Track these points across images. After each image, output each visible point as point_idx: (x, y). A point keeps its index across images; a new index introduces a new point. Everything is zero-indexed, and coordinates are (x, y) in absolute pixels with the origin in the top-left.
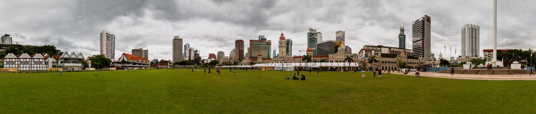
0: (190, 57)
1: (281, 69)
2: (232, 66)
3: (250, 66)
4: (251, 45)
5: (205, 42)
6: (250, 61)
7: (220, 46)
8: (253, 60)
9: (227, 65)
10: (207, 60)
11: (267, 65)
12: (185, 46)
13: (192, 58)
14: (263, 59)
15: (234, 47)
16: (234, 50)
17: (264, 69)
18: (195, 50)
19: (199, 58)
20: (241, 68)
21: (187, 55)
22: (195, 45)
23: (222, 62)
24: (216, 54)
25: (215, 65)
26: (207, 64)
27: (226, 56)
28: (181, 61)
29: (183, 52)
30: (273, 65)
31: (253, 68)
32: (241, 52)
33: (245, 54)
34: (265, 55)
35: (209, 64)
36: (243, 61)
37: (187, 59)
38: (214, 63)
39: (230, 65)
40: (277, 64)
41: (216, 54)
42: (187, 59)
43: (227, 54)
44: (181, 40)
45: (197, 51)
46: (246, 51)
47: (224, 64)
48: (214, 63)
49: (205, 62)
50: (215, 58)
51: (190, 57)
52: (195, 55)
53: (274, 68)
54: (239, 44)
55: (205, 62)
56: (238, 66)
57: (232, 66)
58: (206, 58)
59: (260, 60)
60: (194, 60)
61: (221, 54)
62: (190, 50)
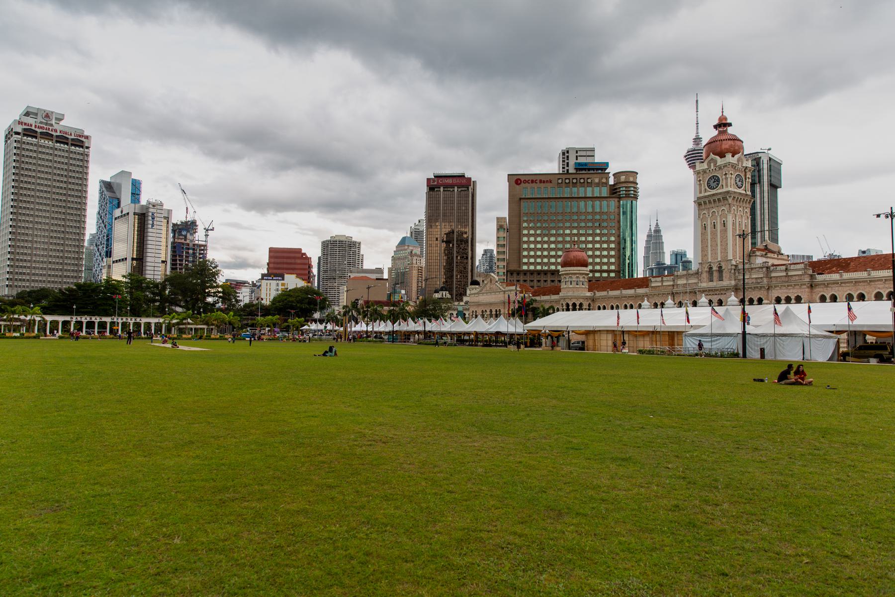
0: (140, 259)
1: (735, 345)
2: (411, 326)
3: (515, 327)
4: (516, 201)
5: (246, 173)
6: (514, 294)
7: (332, 206)
8: (535, 290)
9: (383, 318)
10: (255, 286)
11: (628, 319)
12: (108, 187)
13: (157, 269)
14: (594, 284)
15: (423, 217)
16: (416, 234)
17: (606, 343)
18: (178, 217)
19: (205, 272)
20: (460, 339)
21: (123, 248)
22: (174, 181)
23: (344, 300)
24: (314, 253)
25: (306, 314)
26: (252, 311)
27: (368, 265)
28: (68, 284)
29: (91, 227)
30: (673, 317)
31: (534, 339)
32: (458, 246)
33: (480, 250)
34: (604, 262)
35: (266, 311)
36: (472, 294)
37: (119, 273)
38: (299, 302)
39: (394, 317)
40: (701, 317)
41: (314, 253)
42: (119, 273)
43: (378, 255)
44: (79, 142)
45: (190, 226)
46: (486, 240)
47: (356, 311)
48: (296, 308)
49: (244, 297)
50: (308, 277)
51: (140, 259)
52: (177, 250)
53: (673, 336)
54: (450, 195)
55: (244, 297)
56: (446, 326)
57: (411, 326)
58: (252, 275)
59: (574, 286)
60: (168, 280)
61: (341, 251)
62: (143, 219)
